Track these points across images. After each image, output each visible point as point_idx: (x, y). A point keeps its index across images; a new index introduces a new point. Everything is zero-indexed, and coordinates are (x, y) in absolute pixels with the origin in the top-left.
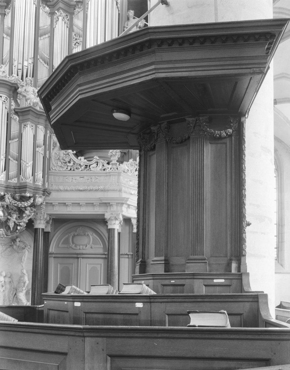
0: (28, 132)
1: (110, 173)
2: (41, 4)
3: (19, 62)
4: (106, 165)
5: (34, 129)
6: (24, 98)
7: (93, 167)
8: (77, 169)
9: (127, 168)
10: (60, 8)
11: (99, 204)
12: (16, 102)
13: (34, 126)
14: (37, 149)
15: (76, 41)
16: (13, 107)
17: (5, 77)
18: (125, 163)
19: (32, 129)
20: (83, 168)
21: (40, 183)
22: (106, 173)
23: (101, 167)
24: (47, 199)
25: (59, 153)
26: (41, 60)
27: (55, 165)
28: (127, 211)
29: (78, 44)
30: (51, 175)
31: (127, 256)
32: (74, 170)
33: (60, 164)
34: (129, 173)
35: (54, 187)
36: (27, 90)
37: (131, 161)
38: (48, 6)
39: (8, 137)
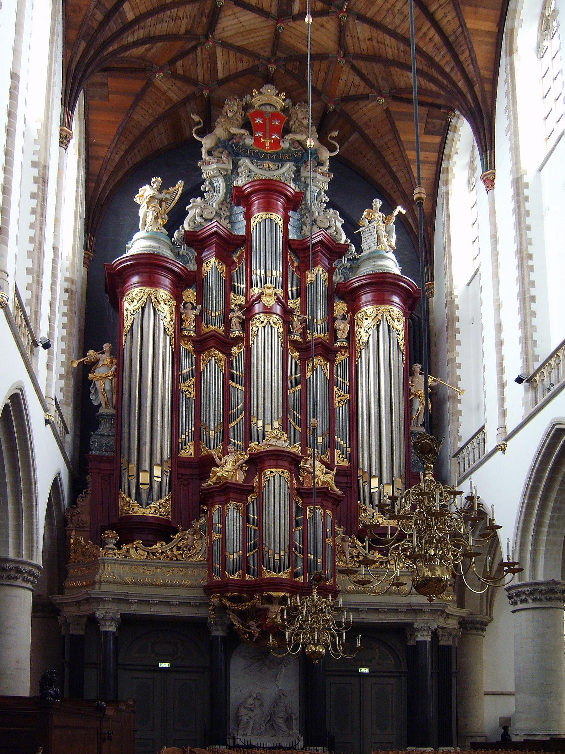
3: (266, 422)
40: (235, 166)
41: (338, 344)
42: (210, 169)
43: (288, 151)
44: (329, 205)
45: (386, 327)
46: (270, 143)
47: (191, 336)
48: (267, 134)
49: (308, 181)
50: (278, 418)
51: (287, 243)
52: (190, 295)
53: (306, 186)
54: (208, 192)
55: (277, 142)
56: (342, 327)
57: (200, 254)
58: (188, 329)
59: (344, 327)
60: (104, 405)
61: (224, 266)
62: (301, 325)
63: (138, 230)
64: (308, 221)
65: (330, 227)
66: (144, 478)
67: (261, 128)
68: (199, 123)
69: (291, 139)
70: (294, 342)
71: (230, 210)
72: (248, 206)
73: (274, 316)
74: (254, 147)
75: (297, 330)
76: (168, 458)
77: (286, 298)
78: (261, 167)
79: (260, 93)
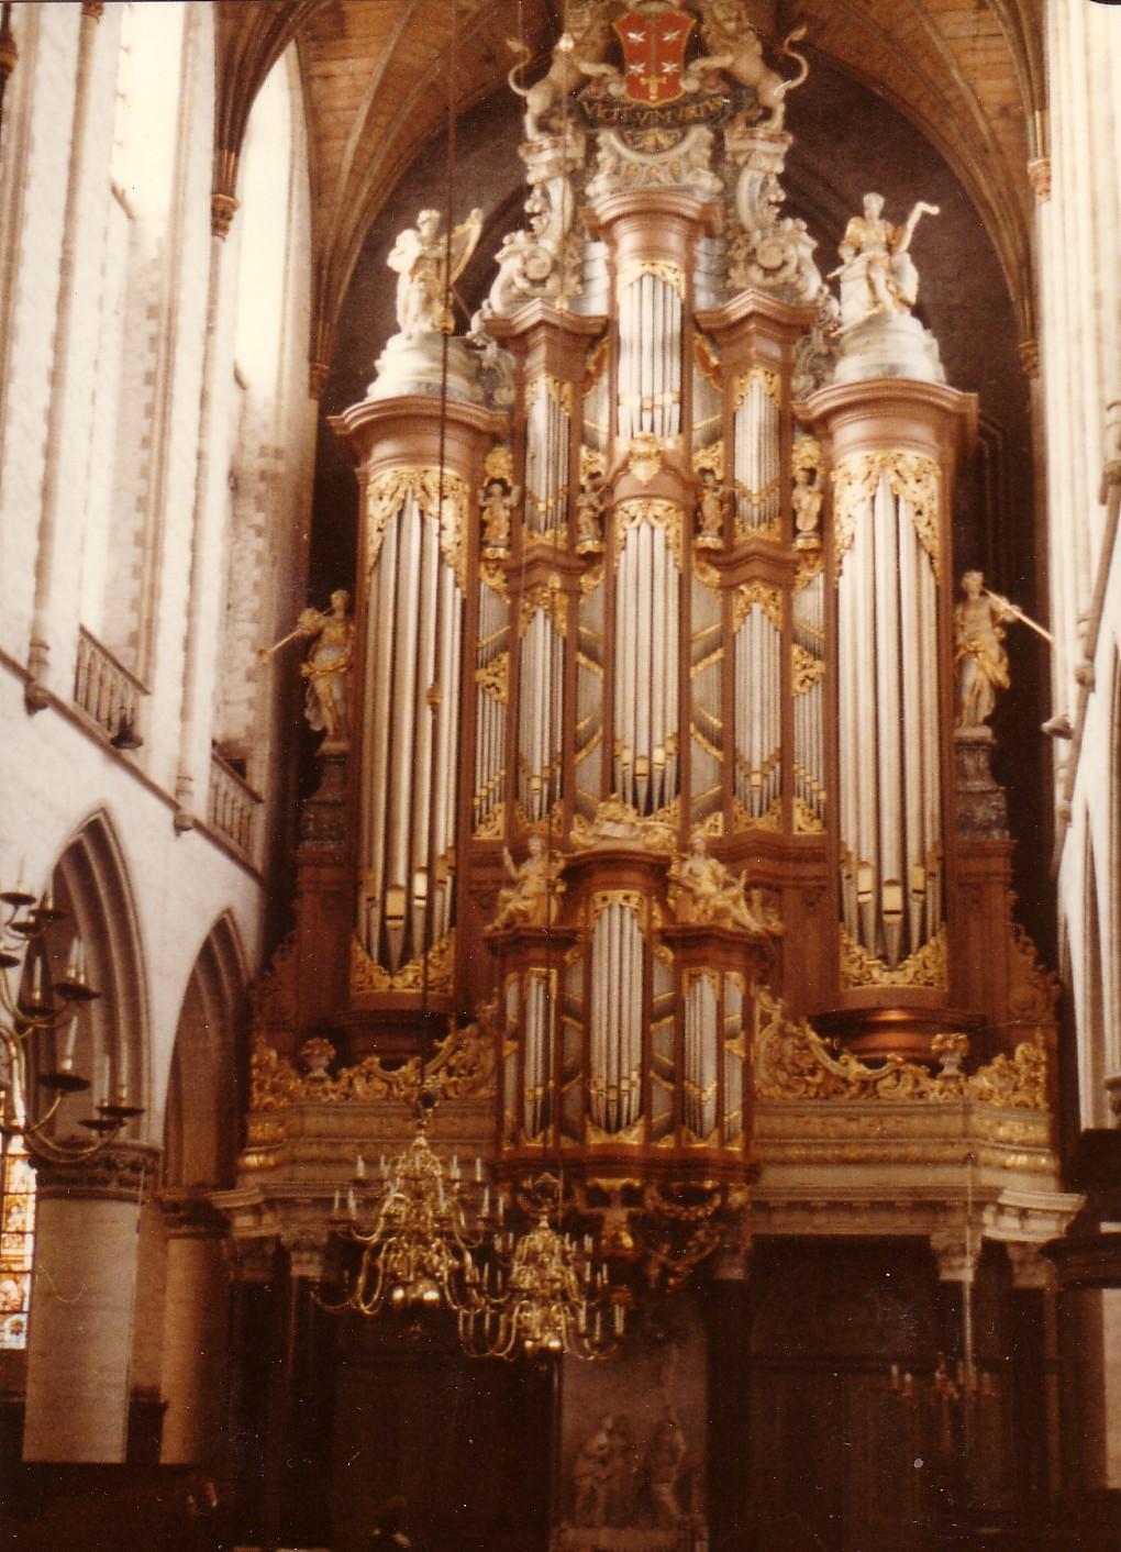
0: (704, 996)
2: (694, 564)
6: (689, 896)
7: (886, 1088)
8: (836, 1092)
14: (727, 1045)
15: (804, 673)
16: (658, 924)
17: (636, 838)
18: (985, 1070)
19: (714, 986)
20: (854, 1089)
21: (736, 1148)
23: (909, 1088)
25: (781, 1046)
26: (699, 736)
29: (812, 680)
32: (827, 1098)
33: (782, 1076)
34: (997, 1102)
35: (771, 1153)
36: (695, 871)
37: (999, 1060)
38: (717, 566)
39: (650, 1014)
40: (592, 148)
41: (800, 543)
42: (542, 160)
43: (695, 97)
44: (788, 210)
46: (660, 86)
48: (653, 68)
49: (740, 160)
50: (664, 740)
51: (690, 318)
53: (738, 170)
54: (539, 214)
55: (674, 80)
56: (807, 502)
57: (521, 363)
58: (493, 542)
59: (810, 504)
60: (331, 732)
61: (567, 387)
62: (722, 509)
63: (396, 330)
64: (741, 255)
65: (784, 263)
66: (396, 904)
67: (640, 53)
69: (703, 70)
70: (707, 550)
71: (582, 251)
72: (613, 244)
73: (659, 501)
74: (629, 99)
75: (712, 523)
76: (447, 849)
77: (689, 449)
78: (641, 145)
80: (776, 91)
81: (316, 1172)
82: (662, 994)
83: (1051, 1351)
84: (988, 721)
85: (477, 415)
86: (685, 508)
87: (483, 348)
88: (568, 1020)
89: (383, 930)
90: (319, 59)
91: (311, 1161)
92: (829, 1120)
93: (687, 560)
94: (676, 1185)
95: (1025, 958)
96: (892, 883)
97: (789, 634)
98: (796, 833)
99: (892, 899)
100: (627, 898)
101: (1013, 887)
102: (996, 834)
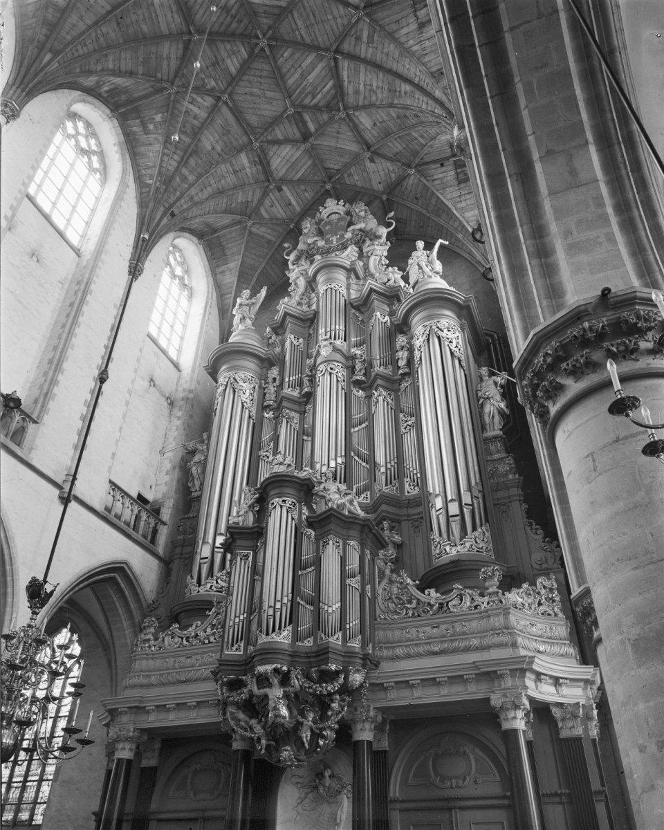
1: (487, 611)
4: (477, 598)
5: (341, 547)
7: (455, 605)
8: (424, 612)
9: (521, 600)
10: (379, 385)
11: (474, 676)
12: (310, 508)
13: (341, 543)
14: (348, 581)
17: (292, 472)
18: (515, 590)
21: (355, 644)
22: (481, 613)
24: (373, 675)
27: (385, 610)
28: (537, 688)
30: (379, 629)
31: (557, 799)
32: (419, 616)
33: (392, 606)
35: (385, 653)
37: (525, 586)
39: (298, 564)
44: (388, 266)
45: (436, 340)
47: (269, 406)
49: (369, 254)
52: (274, 372)
56: (403, 356)
61: (301, 340)
68: (289, 247)
75: (360, 371)
79: (325, 208)
80: (383, 231)
81: (137, 693)
82: (306, 556)
83: (595, 785)
84: (501, 430)
85: (262, 351)
86: (347, 367)
87: (271, 338)
88: (256, 577)
89: (200, 564)
90: (218, 266)
91: (134, 686)
92: (421, 630)
93: (348, 386)
94: (313, 670)
95: (536, 537)
96: (452, 500)
97: (397, 409)
98: (406, 494)
99: (454, 509)
100: (284, 501)
101: (525, 501)
102: (510, 477)
